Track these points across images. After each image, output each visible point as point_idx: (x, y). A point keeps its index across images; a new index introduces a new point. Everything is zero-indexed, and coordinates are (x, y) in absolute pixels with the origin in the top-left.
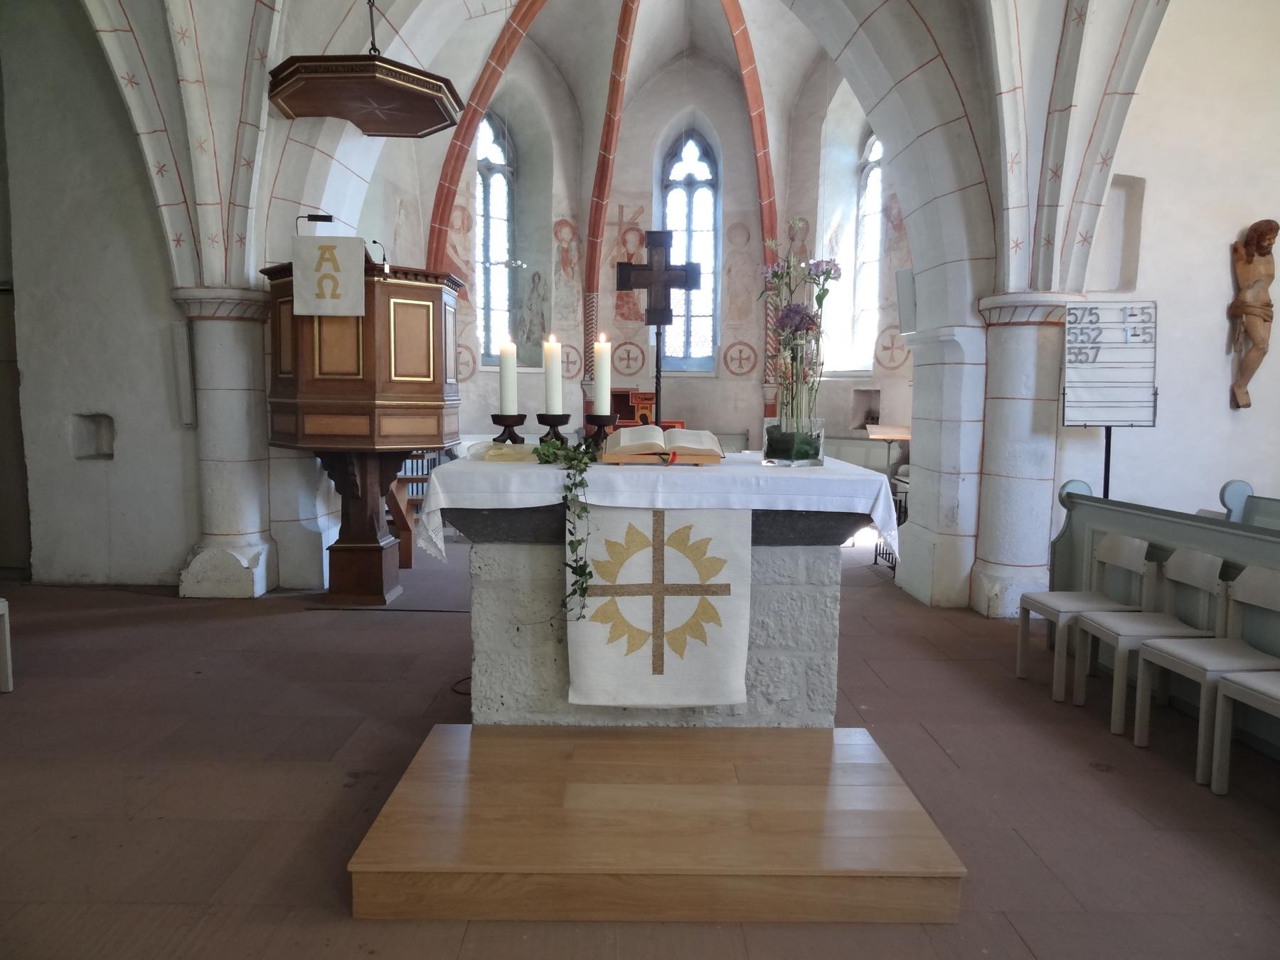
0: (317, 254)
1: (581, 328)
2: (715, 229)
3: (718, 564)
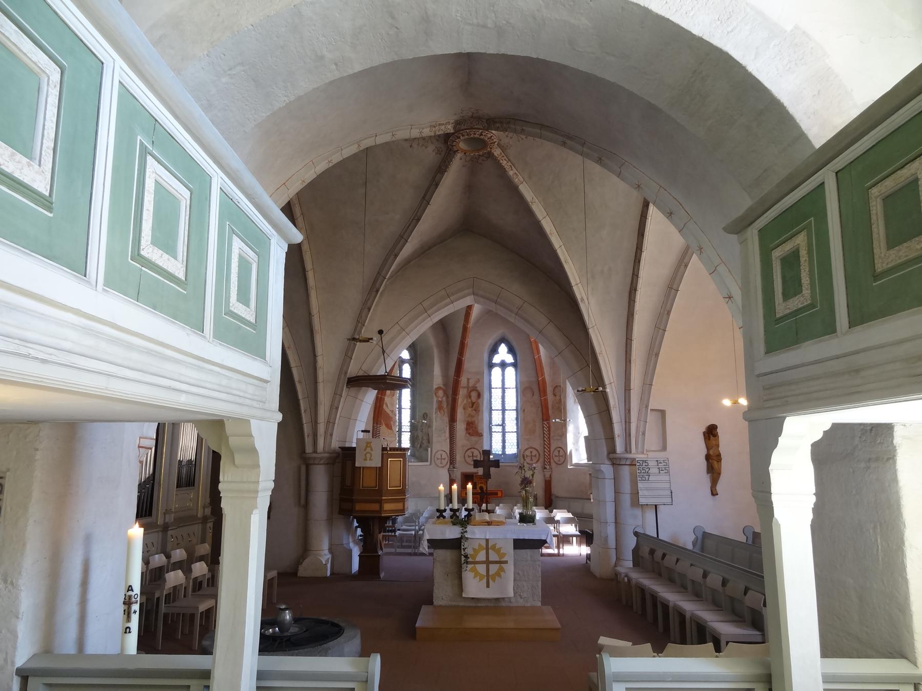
3: (504, 555)
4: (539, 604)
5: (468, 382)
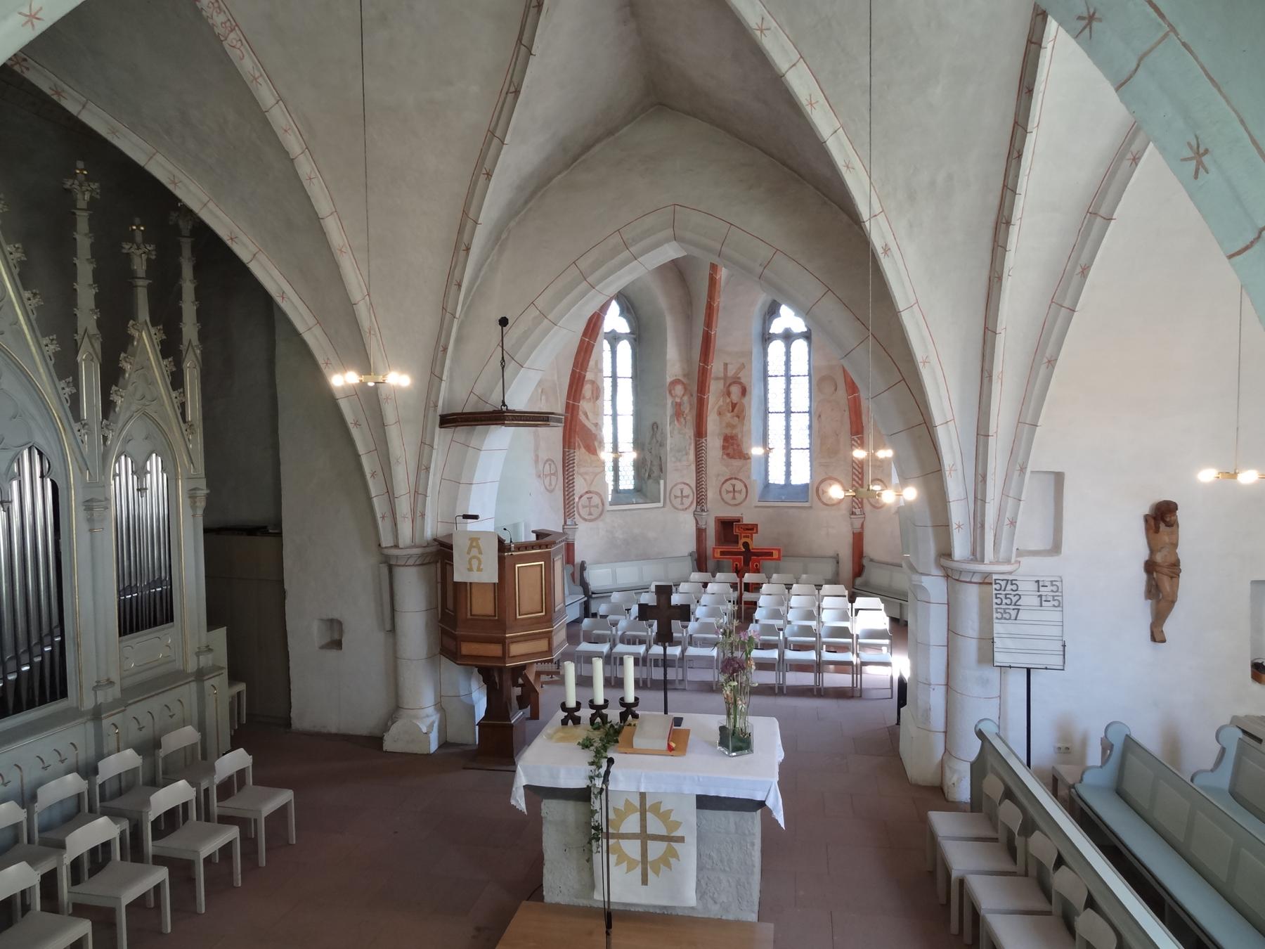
1: (693, 467)
2: (810, 375)
3: (677, 825)
4: (753, 917)
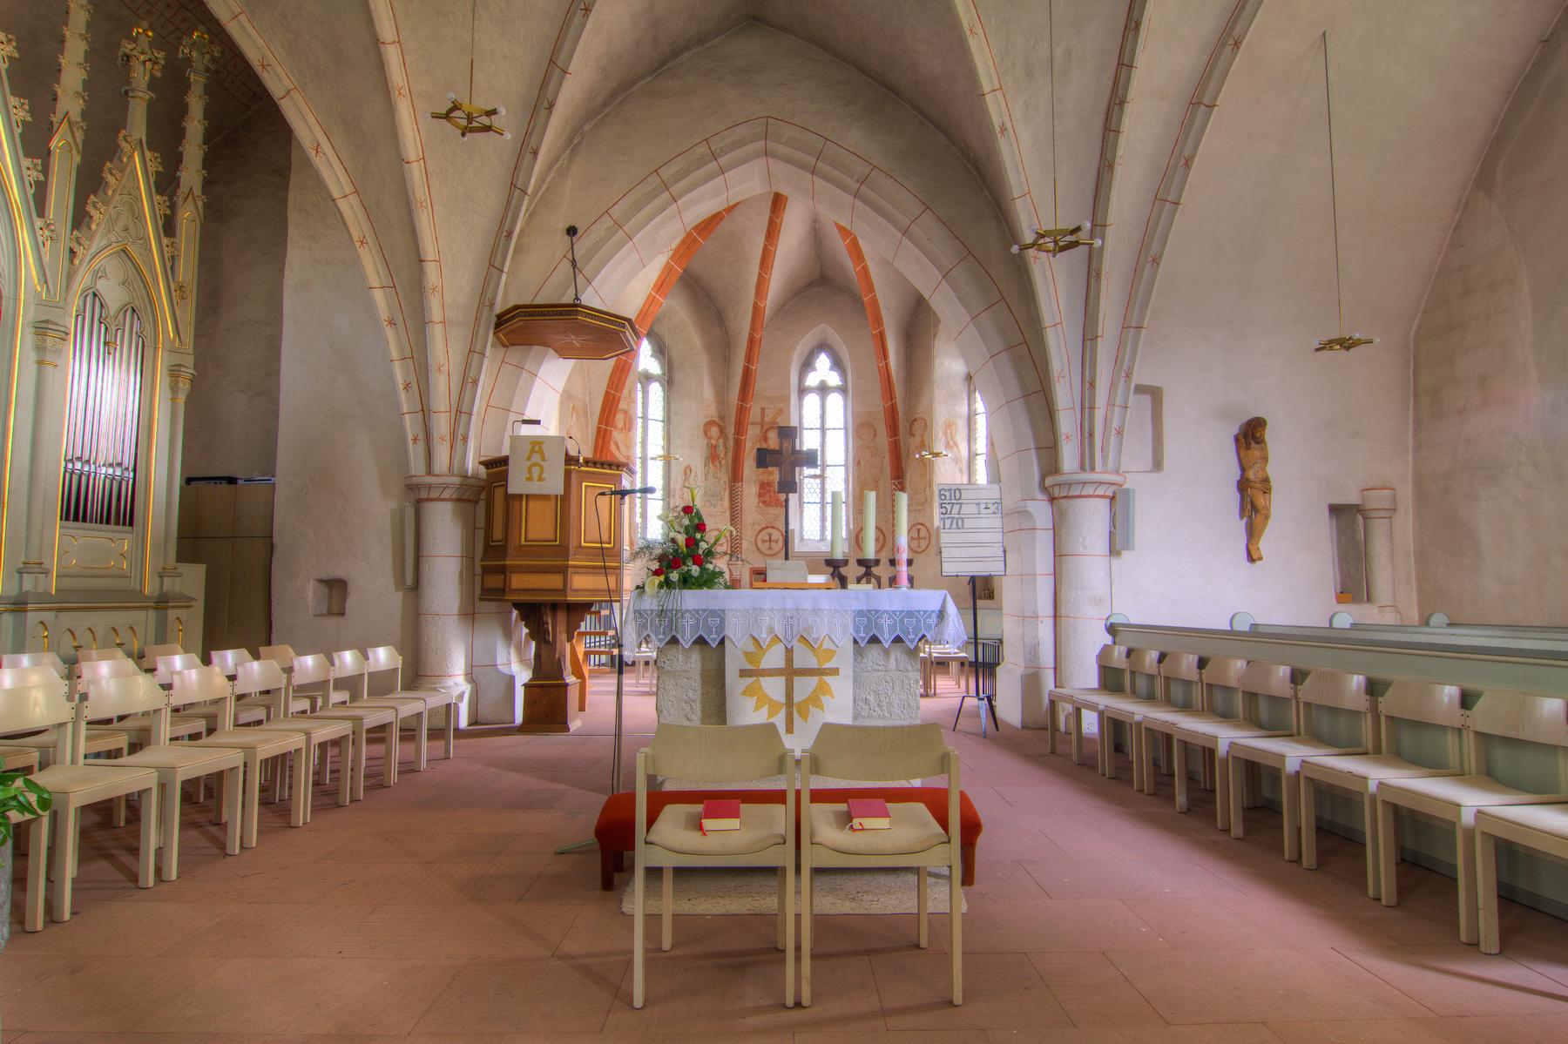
0: (529, 447)
1: (728, 514)
2: (846, 428)
5: (763, 414)
